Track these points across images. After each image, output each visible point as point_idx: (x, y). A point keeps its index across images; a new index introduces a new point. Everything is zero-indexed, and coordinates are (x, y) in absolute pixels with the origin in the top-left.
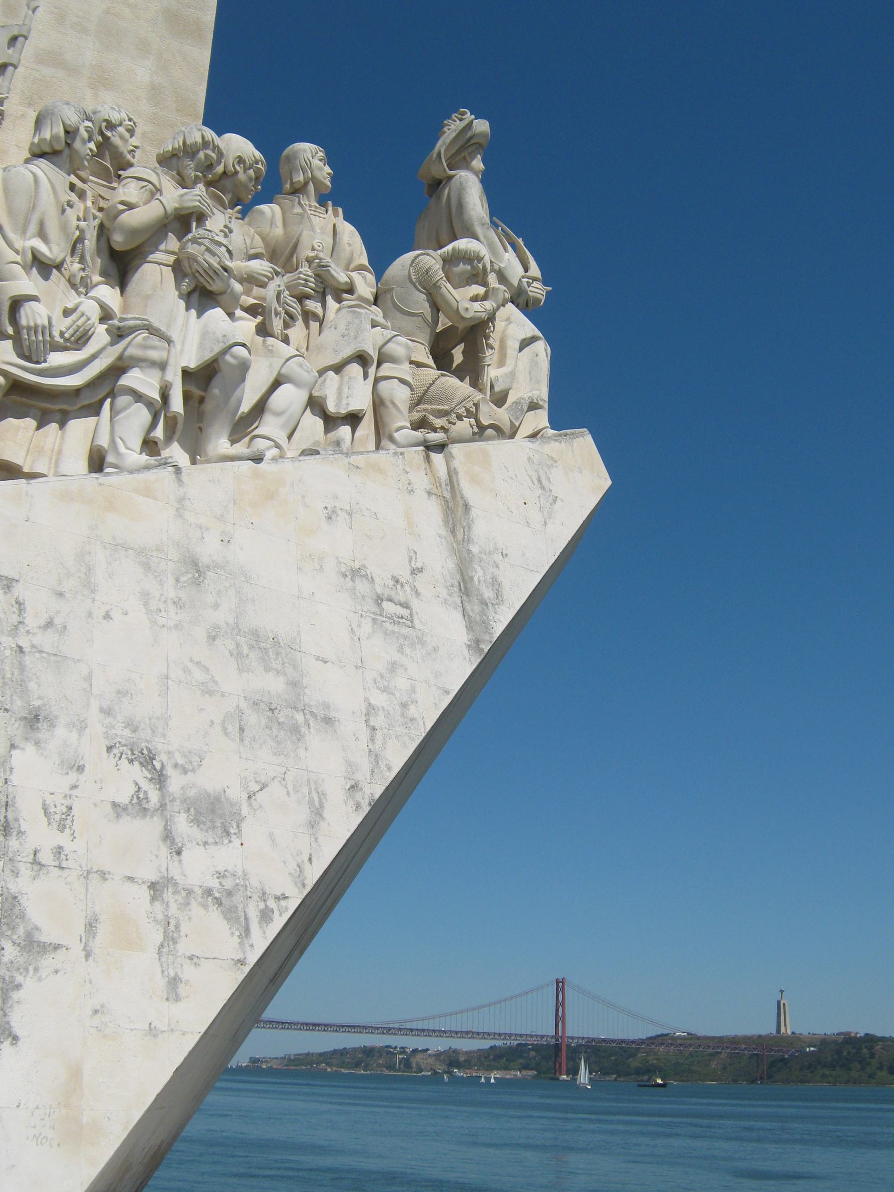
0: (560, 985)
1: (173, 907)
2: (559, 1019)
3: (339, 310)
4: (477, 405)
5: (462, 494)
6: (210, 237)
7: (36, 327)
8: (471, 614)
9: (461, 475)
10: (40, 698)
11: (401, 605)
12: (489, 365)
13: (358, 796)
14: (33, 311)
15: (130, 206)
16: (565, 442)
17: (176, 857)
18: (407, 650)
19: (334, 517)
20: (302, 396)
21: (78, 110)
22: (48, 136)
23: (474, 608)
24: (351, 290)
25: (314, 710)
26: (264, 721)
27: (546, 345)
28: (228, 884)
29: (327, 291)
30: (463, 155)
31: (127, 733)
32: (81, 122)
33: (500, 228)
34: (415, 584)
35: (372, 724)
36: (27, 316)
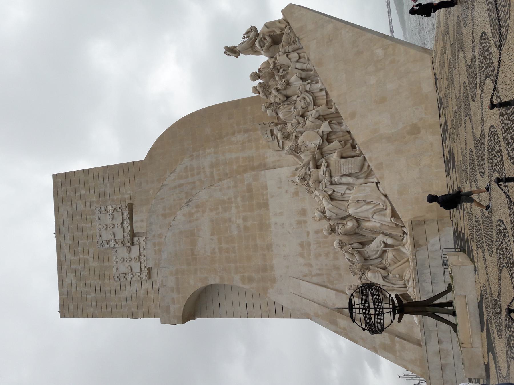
15: (279, 99)
24: (274, 62)
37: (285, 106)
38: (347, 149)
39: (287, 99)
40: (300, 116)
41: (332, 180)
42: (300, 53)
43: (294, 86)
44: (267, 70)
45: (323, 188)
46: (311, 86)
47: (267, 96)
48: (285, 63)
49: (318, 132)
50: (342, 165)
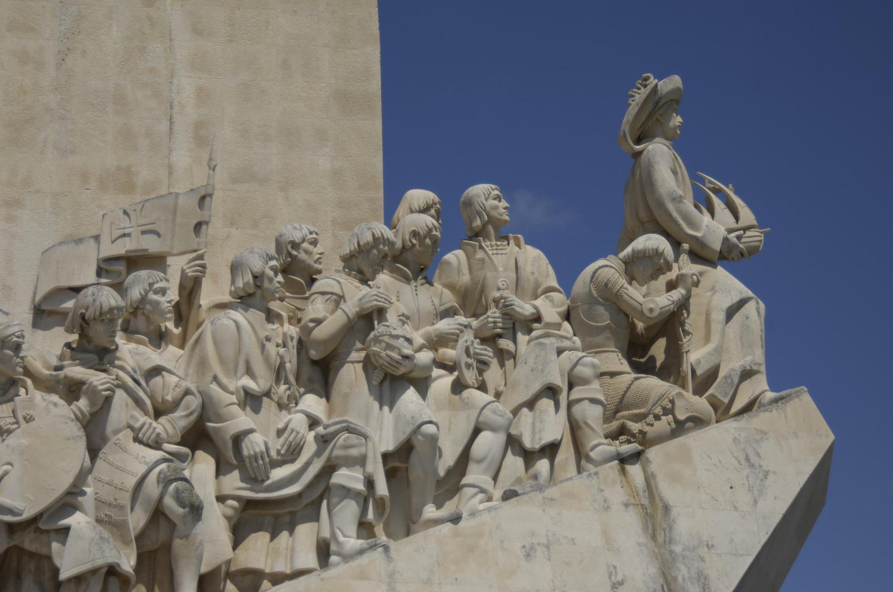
3: (529, 342)
4: (672, 402)
5: (661, 497)
6: (388, 333)
7: (256, 454)
9: (660, 478)
12: (687, 352)
14: (251, 442)
16: (777, 409)
19: (532, 554)
20: (500, 439)
21: (261, 255)
24: (538, 318)
27: (758, 303)
29: (517, 325)
30: (655, 118)
32: (264, 266)
33: (706, 181)
36: (247, 447)
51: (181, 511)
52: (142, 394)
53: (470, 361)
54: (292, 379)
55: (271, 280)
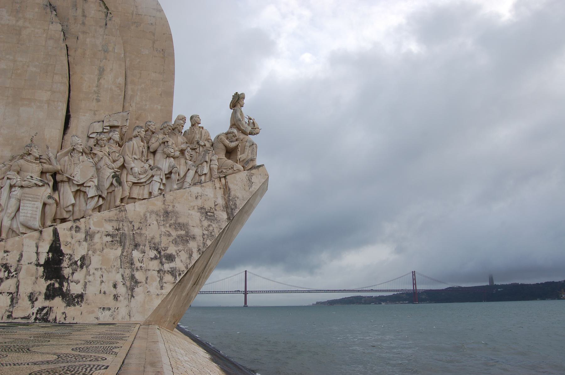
0: (414, 273)
1: (162, 274)
2: (414, 284)
8: (229, 212)
10: (137, 241)
11: (212, 213)
13: (200, 251)
15: (153, 143)
17: (162, 266)
18: (213, 222)
22: (135, 134)
23: (229, 211)
24: (205, 146)
25: (191, 236)
26: (180, 240)
28: (172, 269)
31: (153, 245)
34: (216, 208)
35: (204, 237)
37: (141, 149)
38: (61, 214)
39: (152, 152)
40: (123, 164)
41: (17, 188)
42: (205, 176)
43: (165, 163)
44: (197, 137)
45: (8, 175)
46: (157, 182)
47: (162, 129)
48: (201, 157)
49: (92, 181)
50: (33, 203)
51: (117, 184)
52: (110, 157)
53: (188, 154)
54: (146, 156)
55: (142, 133)
